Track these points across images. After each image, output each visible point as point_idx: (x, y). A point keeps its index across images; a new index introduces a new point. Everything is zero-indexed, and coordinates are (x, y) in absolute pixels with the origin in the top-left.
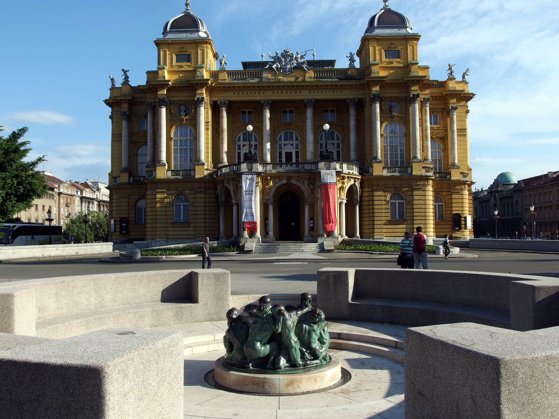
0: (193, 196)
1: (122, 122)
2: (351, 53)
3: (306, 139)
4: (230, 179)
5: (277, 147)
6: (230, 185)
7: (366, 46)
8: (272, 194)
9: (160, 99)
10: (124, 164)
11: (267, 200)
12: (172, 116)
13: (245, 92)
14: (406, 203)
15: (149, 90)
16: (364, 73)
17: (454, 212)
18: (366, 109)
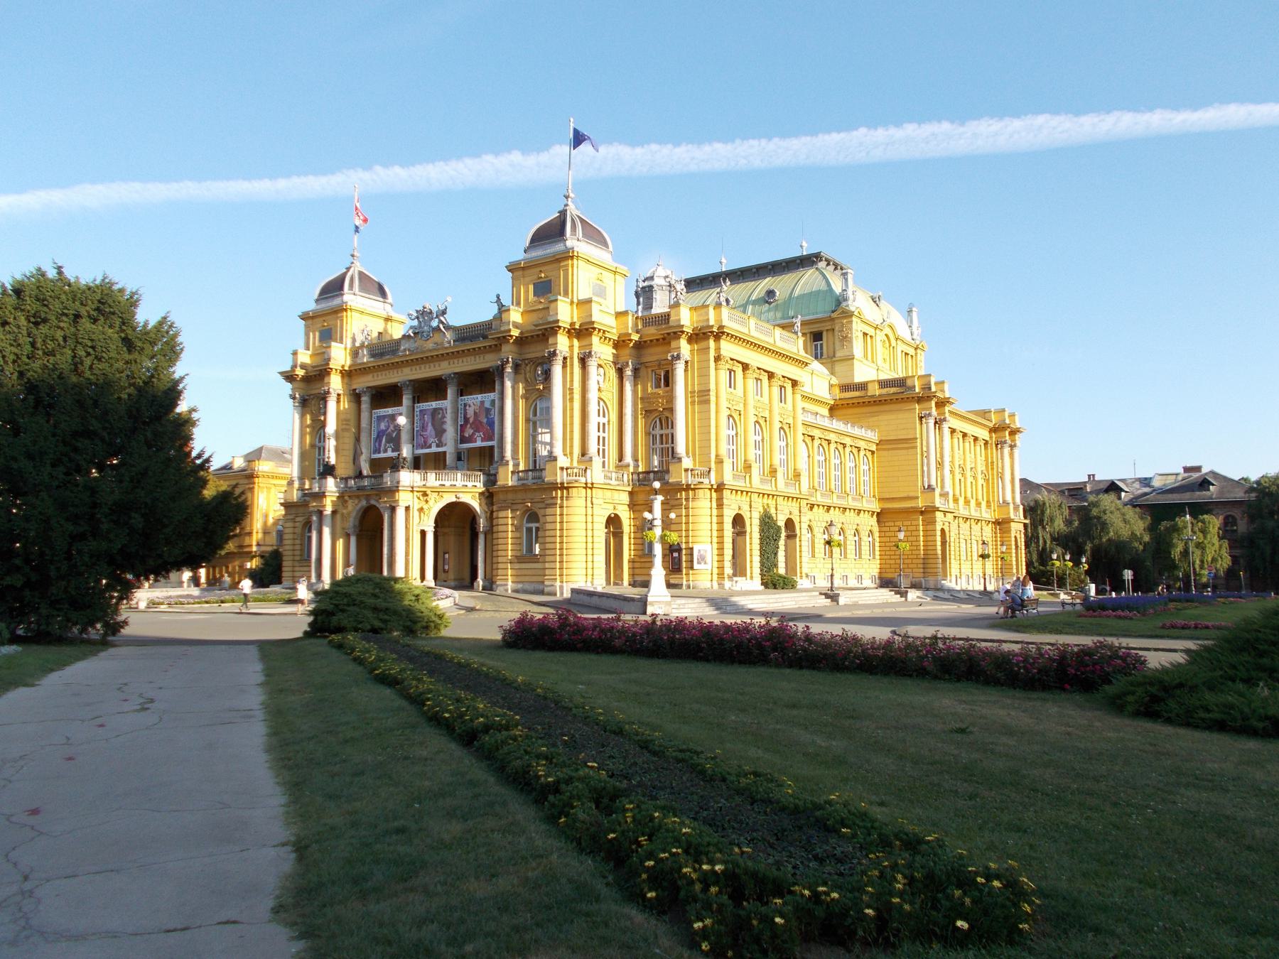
8: (351, 520)
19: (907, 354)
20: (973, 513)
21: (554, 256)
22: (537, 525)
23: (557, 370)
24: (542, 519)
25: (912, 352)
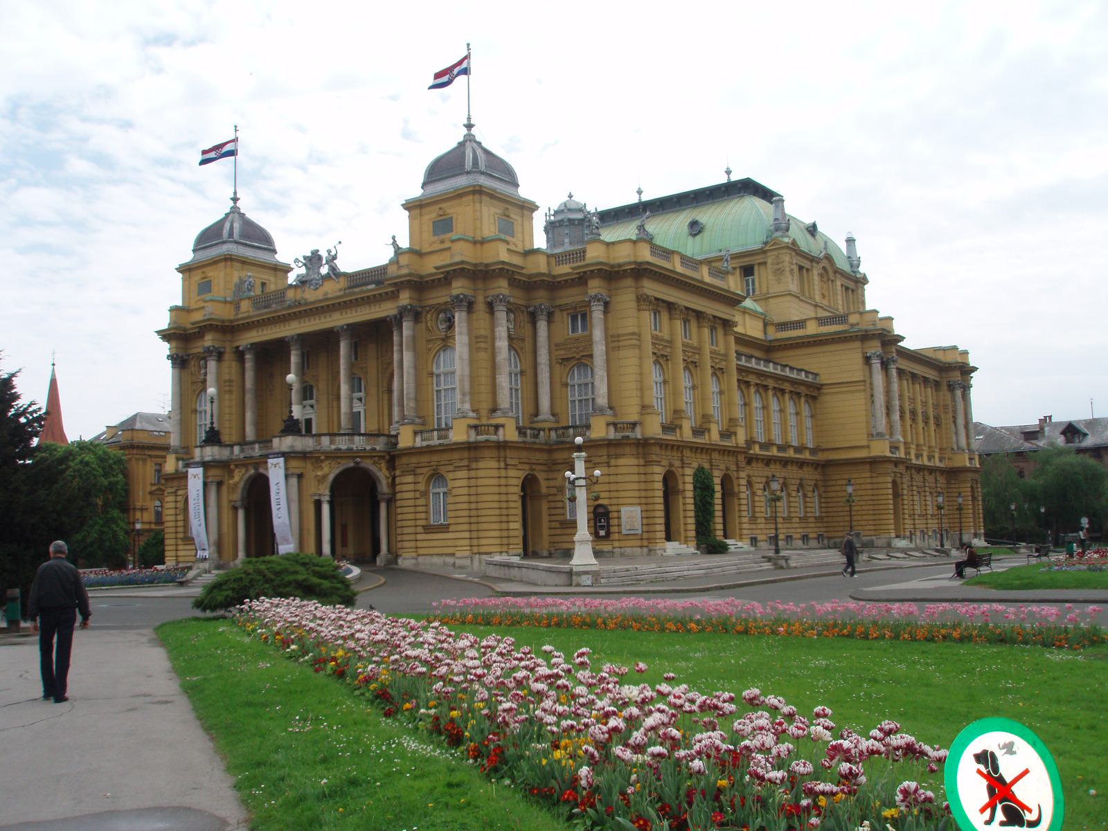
8: (239, 491)
11: (320, 495)
19: (847, 289)
20: (926, 463)
21: (455, 191)
22: (445, 490)
23: (460, 317)
24: (451, 484)
25: (851, 285)
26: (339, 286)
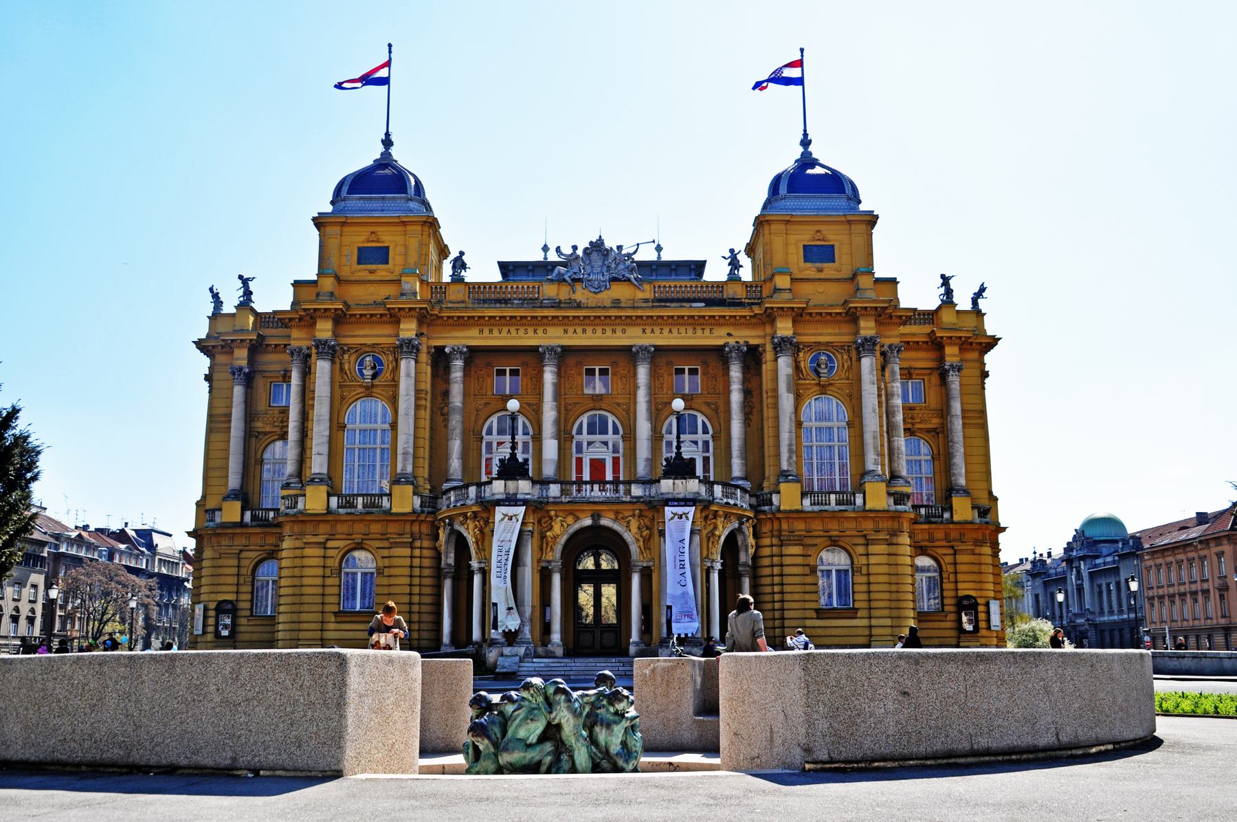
0: (385, 552)
1: (233, 388)
2: (732, 251)
3: (635, 431)
4: (469, 514)
5: (571, 449)
6: (467, 529)
7: (764, 235)
8: (559, 548)
9: (320, 341)
10: (234, 482)
11: (549, 562)
12: (346, 378)
13: (505, 330)
14: (853, 571)
15: (297, 320)
16: (761, 292)
17: (961, 593)
18: (766, 368)
26: (640, 295)
